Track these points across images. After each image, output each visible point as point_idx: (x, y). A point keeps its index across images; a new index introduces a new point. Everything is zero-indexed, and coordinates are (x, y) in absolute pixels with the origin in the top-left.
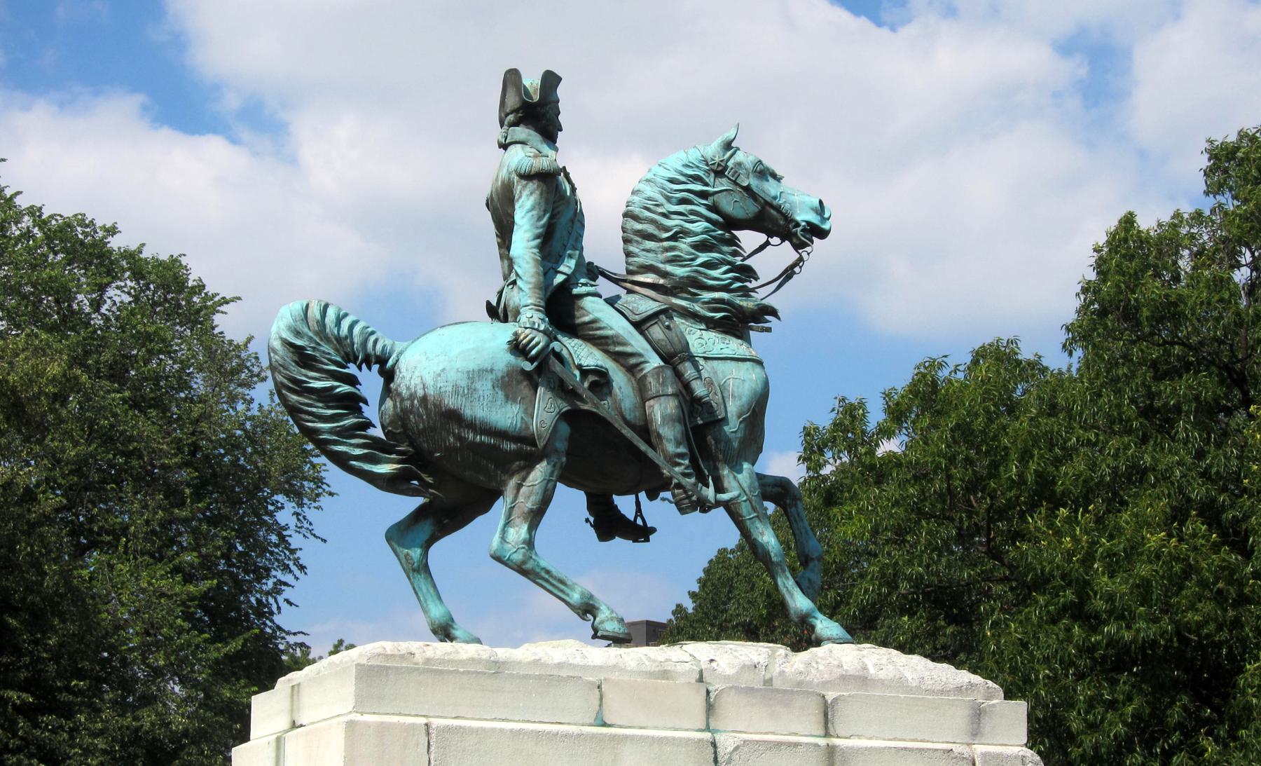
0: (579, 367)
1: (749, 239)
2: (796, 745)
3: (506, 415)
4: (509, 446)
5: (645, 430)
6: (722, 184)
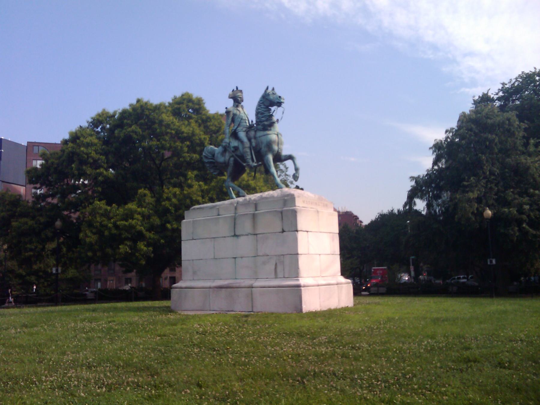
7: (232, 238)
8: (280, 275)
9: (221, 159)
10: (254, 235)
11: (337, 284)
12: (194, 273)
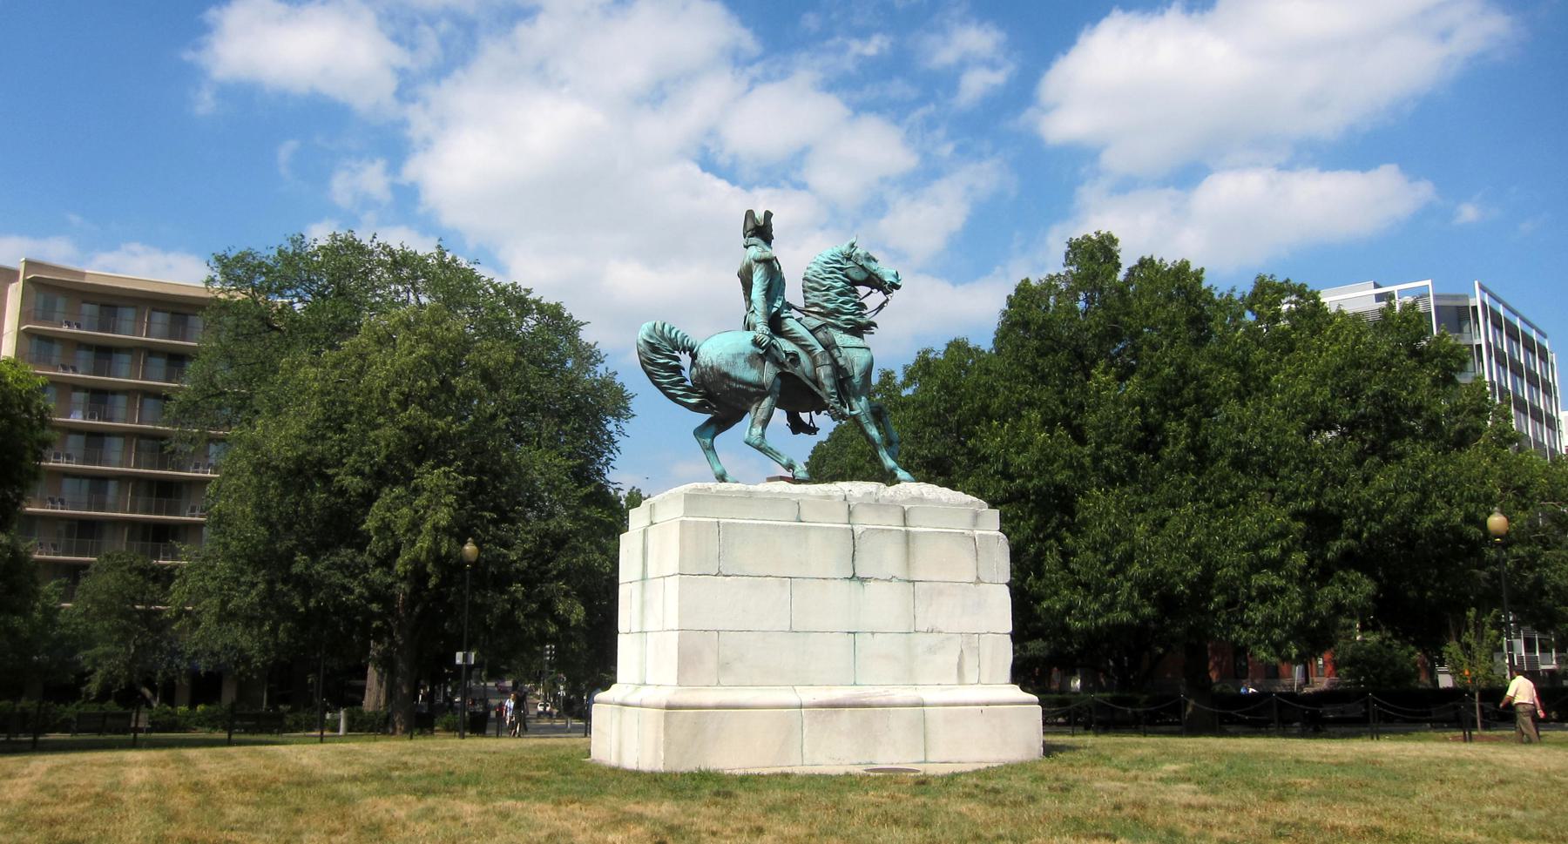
0: (785, 352)
1: (862, 290)
3: (751, 375)
4: (752, 390)
5: (816, 381)
6: (850, 264)
7: (848, 581)
8: (971, 676)
10: (909, 581)
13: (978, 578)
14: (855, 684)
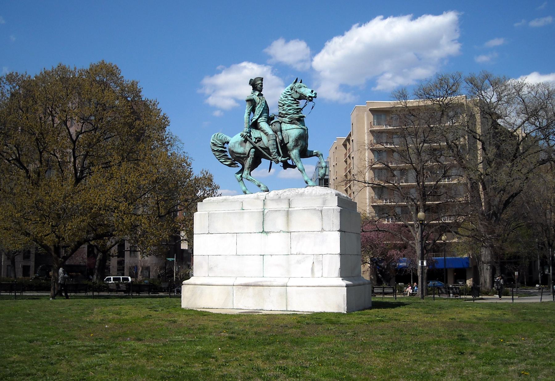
2: (280, 210)
4: (242, 156)
7: (260, 233)
8: (318, 273)
9: (240, 150)
10: (288, 232)
11: (364, 285)
12: (210, 269)
13: (322, 229)
14: (263, 277)
